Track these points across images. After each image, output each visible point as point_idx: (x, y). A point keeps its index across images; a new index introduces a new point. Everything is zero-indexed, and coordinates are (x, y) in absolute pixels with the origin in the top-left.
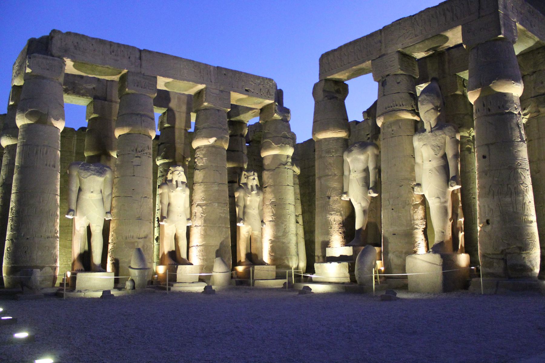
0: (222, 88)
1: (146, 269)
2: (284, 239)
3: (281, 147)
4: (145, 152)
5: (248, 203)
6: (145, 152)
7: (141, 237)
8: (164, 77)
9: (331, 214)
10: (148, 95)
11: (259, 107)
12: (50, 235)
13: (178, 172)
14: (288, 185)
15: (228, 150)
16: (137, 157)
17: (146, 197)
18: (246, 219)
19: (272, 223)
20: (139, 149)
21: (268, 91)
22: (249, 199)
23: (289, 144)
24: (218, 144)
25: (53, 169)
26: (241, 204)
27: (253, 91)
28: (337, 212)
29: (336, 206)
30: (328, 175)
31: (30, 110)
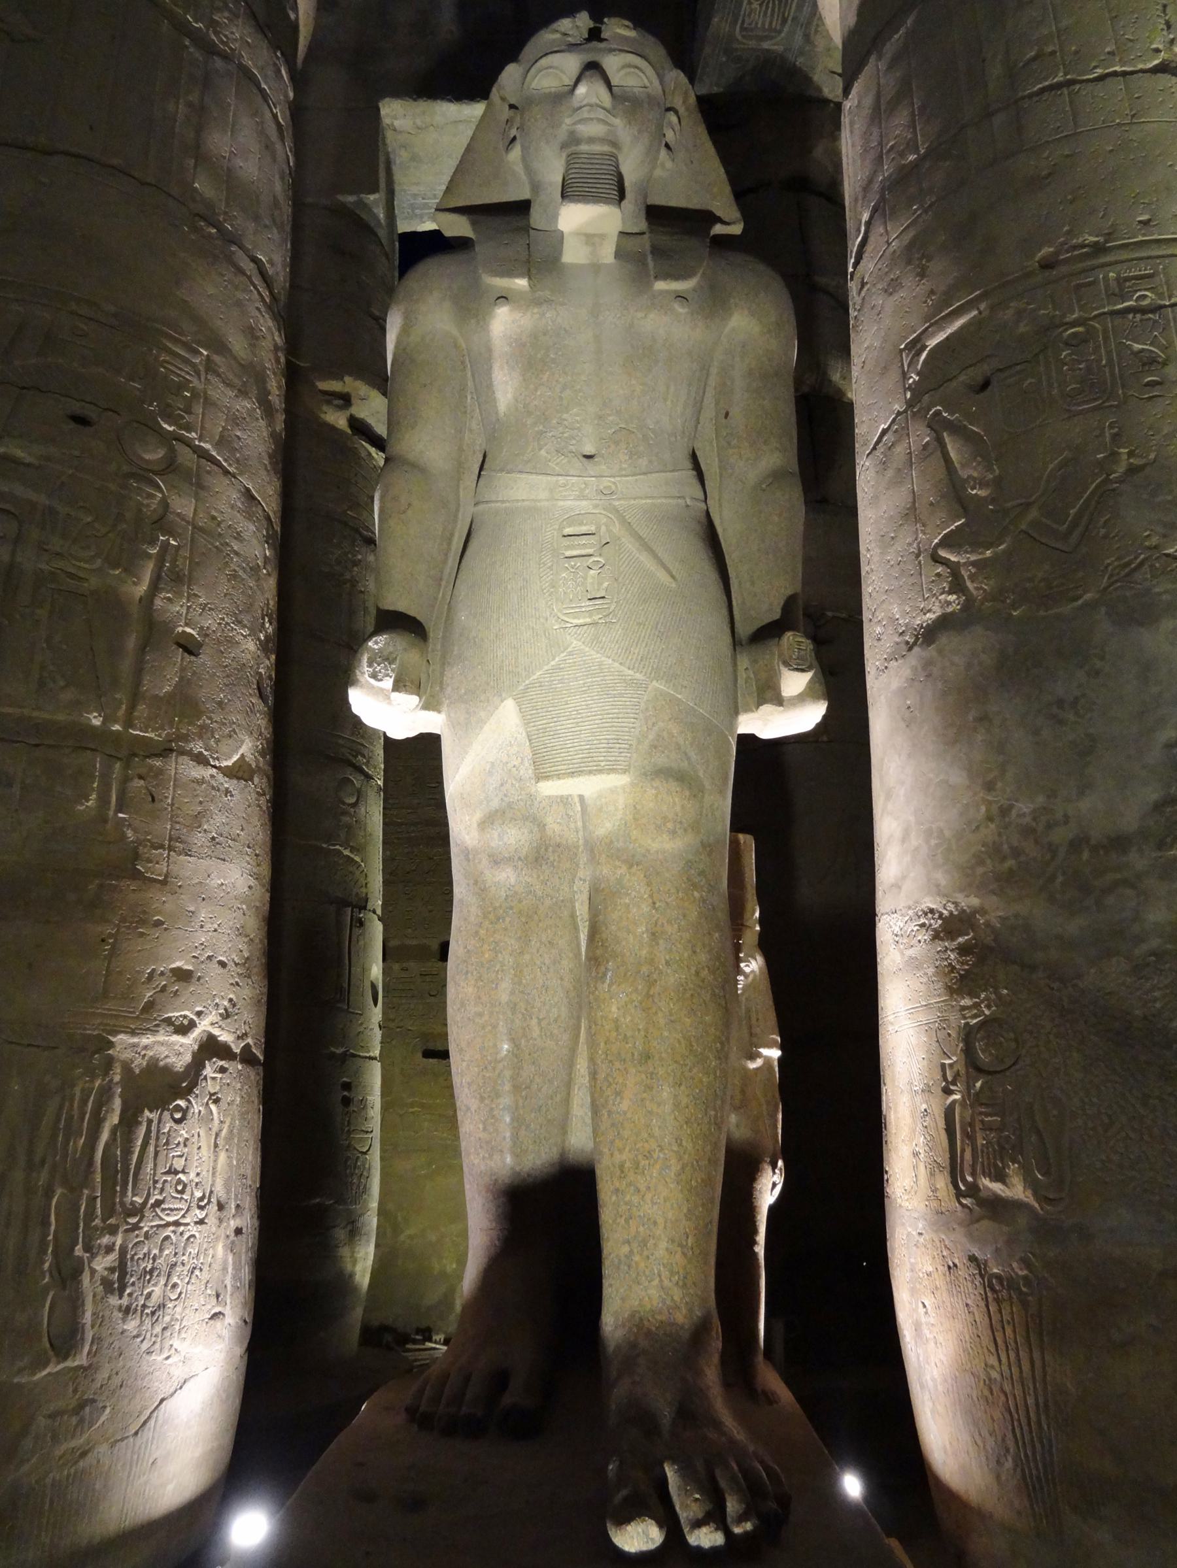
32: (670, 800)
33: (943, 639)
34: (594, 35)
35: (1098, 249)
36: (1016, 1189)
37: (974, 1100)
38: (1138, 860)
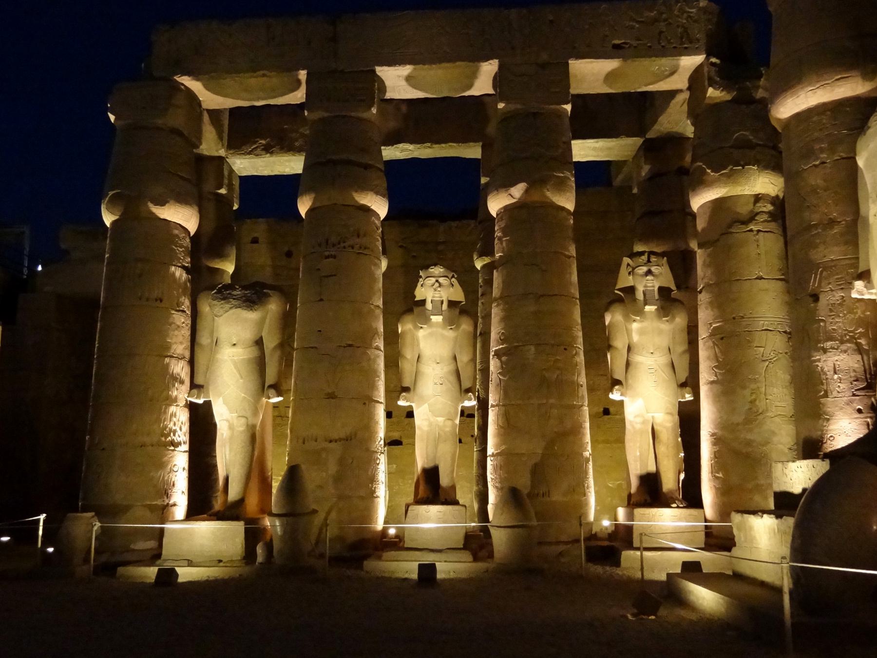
0: (544, 57)
1: (299, 515)
2: (750, 430)
3: (731, 178)
4: (346, 244)
5: (635, 338)
6: (346, 244)
7: (335, 436)
8: (389, 65)
9: (825, 351)
10: (353, 114)
11: (679, 82)
12: (147, 440)
13: (434, 280)
14: (761, 278)
15: (576, 213)
16: (327, 257)
17: (350, 346)
18: (630, 381)
19: (716, 387)
20: (334, 239)
21: (686, 30)
22: (635, 326)
23: (756, 162)
24: (536, 197)
25: (158, 303)
26: (620, 343)
27: (634, 43)
28: (842, 342)
29: (838, 324)
30: (810, 227)
31: (111, 193)
32: (669, 418)
33: (714, 385)
34: (649, 261)
35: (743, 317)
36: (720, 475)
37: (716, 462)
38: (740, 427)
